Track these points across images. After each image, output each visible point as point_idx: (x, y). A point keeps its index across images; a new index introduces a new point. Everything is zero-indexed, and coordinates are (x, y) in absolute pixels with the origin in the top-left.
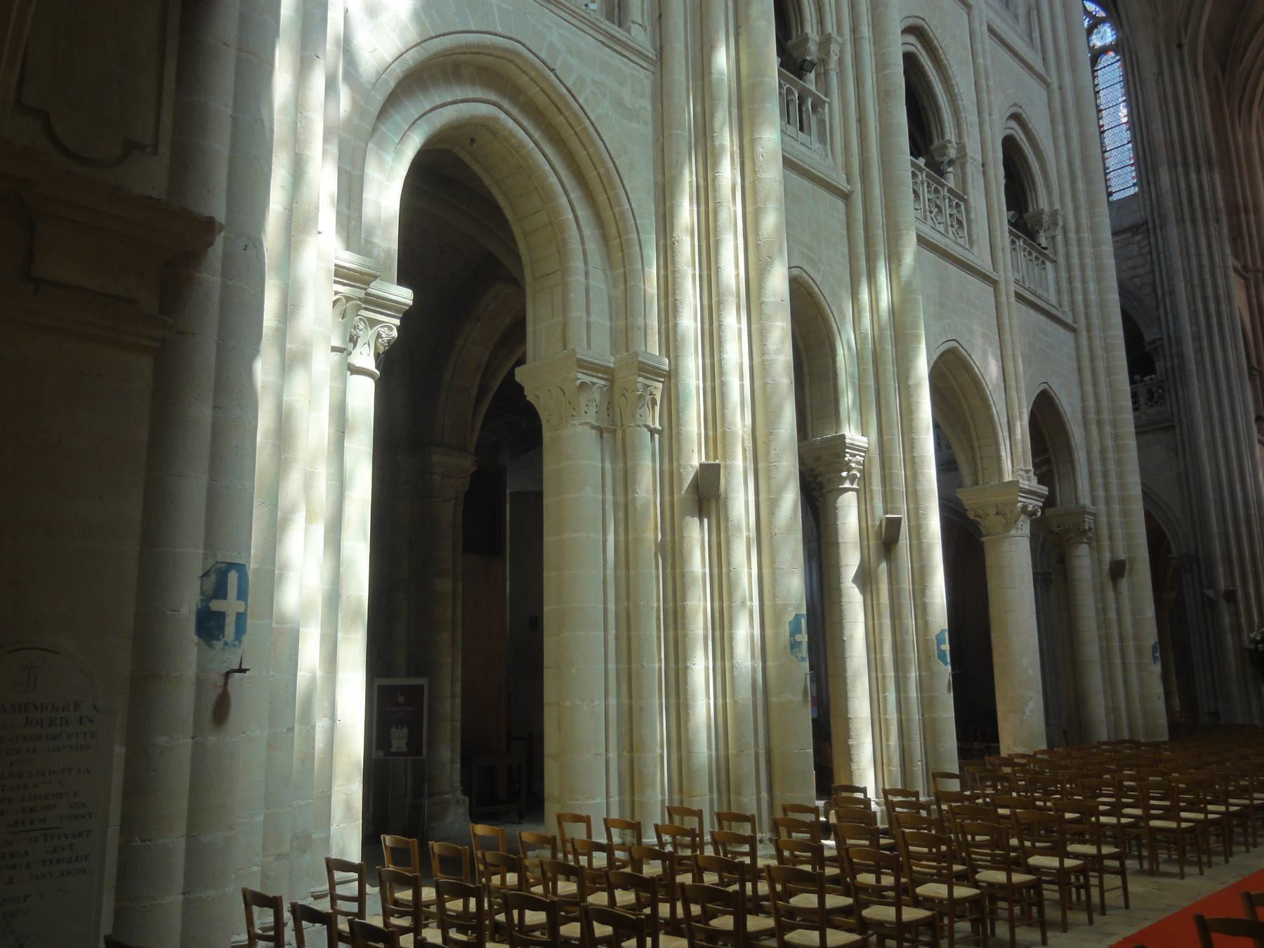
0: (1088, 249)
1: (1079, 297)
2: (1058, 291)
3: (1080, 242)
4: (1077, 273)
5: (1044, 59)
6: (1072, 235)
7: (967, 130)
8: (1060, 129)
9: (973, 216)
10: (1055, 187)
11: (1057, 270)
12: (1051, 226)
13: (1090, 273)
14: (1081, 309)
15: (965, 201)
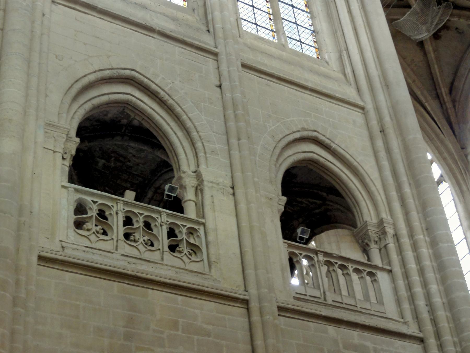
0: (425, 251)
1: (421, 303)
2: (398, 302)
3: (415, 247)
4: (415, 278)
5: (358, 90)
6: (406, 241)
7: (206, 158)
8: (380, 143)
9: (211, 238)
10: (380, 198)
11: (393, 280)
12: (382, 236)
13: (431, 275)
14: (425, 315)
15: (204, 225)
